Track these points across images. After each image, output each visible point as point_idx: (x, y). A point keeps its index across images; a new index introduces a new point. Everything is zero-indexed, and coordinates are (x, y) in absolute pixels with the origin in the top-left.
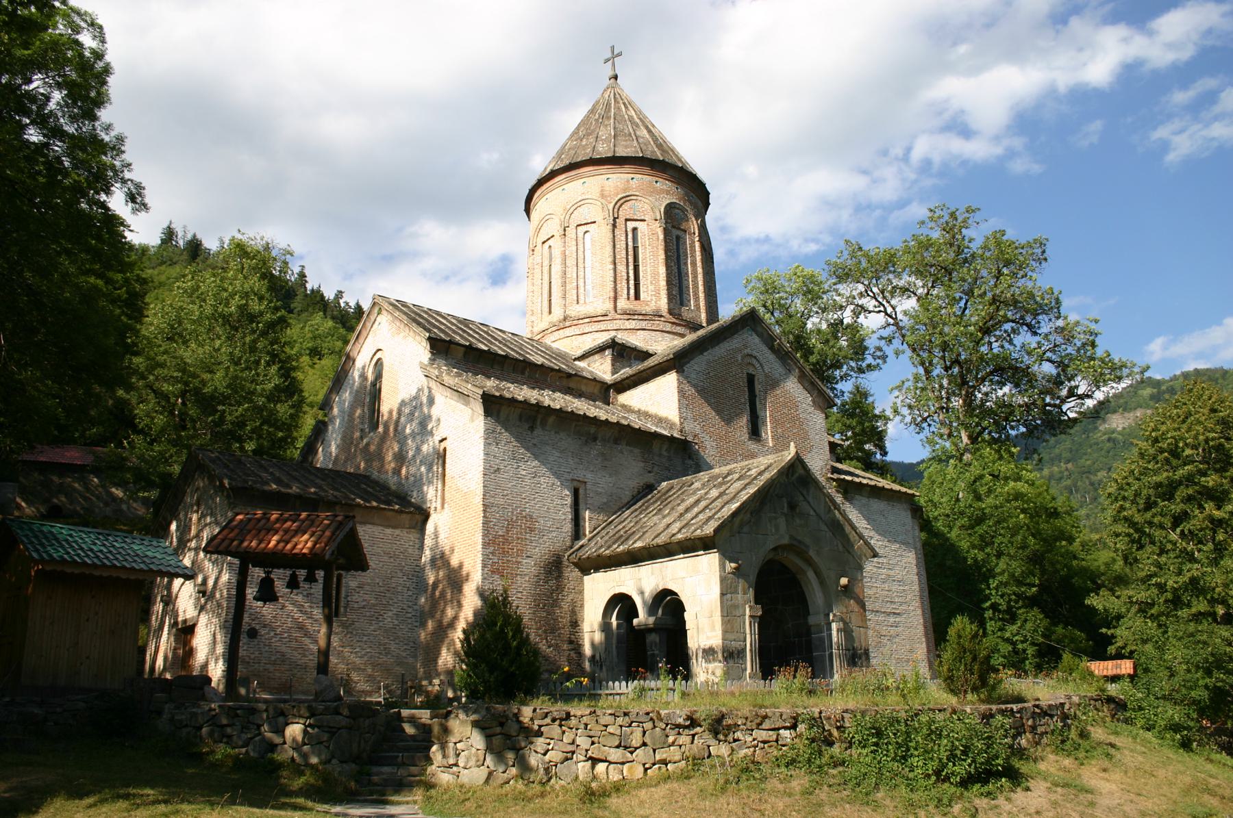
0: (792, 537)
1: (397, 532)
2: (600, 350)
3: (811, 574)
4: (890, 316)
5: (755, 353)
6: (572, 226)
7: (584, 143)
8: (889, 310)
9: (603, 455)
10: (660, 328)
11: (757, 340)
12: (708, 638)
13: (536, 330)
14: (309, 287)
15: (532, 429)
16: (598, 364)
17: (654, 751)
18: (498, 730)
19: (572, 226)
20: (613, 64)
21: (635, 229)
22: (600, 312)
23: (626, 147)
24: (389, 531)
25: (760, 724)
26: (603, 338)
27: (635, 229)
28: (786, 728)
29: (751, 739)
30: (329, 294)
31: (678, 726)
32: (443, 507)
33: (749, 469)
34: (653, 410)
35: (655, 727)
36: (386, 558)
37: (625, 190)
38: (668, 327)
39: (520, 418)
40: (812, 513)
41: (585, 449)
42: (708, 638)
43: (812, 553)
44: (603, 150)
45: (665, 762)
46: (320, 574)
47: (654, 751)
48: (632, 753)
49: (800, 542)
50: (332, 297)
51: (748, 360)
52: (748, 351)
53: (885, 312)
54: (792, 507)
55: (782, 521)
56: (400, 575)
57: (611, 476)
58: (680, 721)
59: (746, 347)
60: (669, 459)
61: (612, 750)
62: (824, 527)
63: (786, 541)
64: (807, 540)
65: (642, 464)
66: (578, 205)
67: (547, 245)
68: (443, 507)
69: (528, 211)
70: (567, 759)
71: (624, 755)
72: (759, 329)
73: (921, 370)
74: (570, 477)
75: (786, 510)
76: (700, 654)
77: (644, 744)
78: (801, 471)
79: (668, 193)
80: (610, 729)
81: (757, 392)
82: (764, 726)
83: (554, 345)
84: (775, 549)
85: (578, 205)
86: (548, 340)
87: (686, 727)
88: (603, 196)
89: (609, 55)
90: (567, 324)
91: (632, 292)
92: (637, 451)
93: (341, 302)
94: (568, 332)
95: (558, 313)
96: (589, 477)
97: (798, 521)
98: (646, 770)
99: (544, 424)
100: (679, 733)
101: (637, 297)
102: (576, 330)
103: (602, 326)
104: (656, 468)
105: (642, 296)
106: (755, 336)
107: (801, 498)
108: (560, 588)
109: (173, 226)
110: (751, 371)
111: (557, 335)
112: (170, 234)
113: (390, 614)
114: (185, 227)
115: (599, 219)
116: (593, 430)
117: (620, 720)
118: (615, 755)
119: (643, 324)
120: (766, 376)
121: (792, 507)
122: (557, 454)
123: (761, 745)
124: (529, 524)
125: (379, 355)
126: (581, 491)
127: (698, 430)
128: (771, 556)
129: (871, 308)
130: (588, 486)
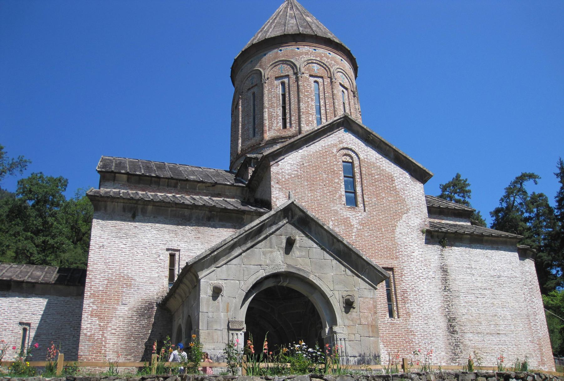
1: (68, 299)
5: (350, 146)
24: (61, 298)
39: (124, 209)
49: (299, 269)
51: (345, 151)
72: (355, 128)
74: (166, 247)
79: (307, 54)
91: (281, 124)
96: (182, 246)
99: (144, 212)
116: (187, 212)
122: (155, 232)
124: (127, 282)
126: (177, 257)
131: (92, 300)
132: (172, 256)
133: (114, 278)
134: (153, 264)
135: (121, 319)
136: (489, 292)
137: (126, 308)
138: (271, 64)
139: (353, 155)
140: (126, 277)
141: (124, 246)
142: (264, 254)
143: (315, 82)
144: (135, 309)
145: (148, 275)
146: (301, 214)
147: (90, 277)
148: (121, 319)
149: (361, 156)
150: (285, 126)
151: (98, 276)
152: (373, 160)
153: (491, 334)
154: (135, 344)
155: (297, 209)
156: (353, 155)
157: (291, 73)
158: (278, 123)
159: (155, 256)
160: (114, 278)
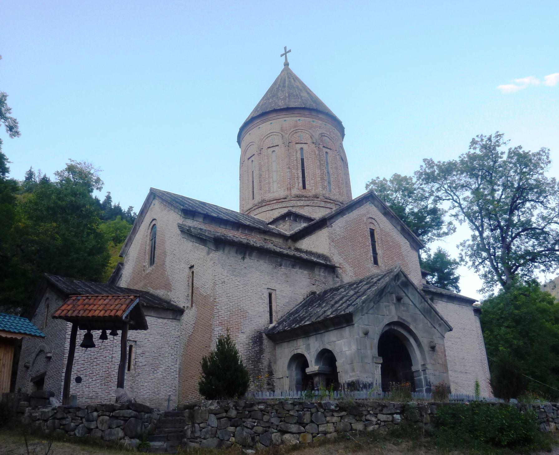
0: (399, 317)
1: (165, 321)
2: (283, 218)
3: (412, 341)
4: (456, 202)
5: (374, 217)
6: (265, 148)
7: (271, 101)
8: (455, 197)
9: (285, 274)
10: (318, 205)
11: (375, 209)
12: (351, 377)
13: (245, 209)
14: (113, 204)
15: (243, 258)
16: (281, 226)
17: (318, 426)
18: (224, 415)
19: (265, 148)
20: (286, 57)
21: (302, 149)
22: (282, 196)
23: (295, 102)
25: (382, 410)
26: (285, 211)
27: (302, 149)
28: (397, 413)
29: (376, 420)
30: (125, 208)
31: (333, 411)
32: (192, 306)
33: (372, 279)
34: (314, 250)
35: (318, 411)
36: (158, 337)
37: (295, 127)
38: (323, 204)
40: (411, 303)
41: (276, 271)
42: (351, 377)
43: (412, 327)
44: (281, 104)
45: (325, 433)
46: (120, 332)
47: (318, 426)
48: (304, 427)
49: (404, 320)
50: (126, 210)
51: (370, 220)
52: (370, 216)
53: (453, 199)
54: (399, 299)
55: (393, 308)
56: (167, 346)
57: (290, 286)
58: (333, 407)
59: (368, 213)
60: (325, 277)
61: (293, 425)
62: (419, 312)
63: (396, 319)
64: (409, 320)
65: (309, 280)
66: (268, 136)
67: (250, 160)
68: (192, 306)
69: (239, 142)
70: (266, 431)
71: (299, 428)
73: (477, 233)
75: (395, 301)
76: (346, 386)
77: (312, 422)
78: (403, 279)
79: (320, 127)
80: (291, 413)
81: (376, 240)
82: (384, 412)
83: (255, 217)
84: (389, 324)
85: (268, 136)
86: (252, 215)
87: (336, 411)
88: (282, 130)
89: (284, 52)
90: (264, 204)
91: (301, 185)
92: (306, 272)
93: (132, 212)
94: (264, 209)
95: (258, 199)
96: (277, 287)
97: (402, 308)
98: (313, 437)
100: (333, 416)
101: (304, 187)
102: (269, 208)
103: (284, 205)
104: (317, 283)
105: (307, 186)
106: (373, 207)
107: (404, 295)
108: (261, 351)
109: (32, 170)
110: (372, 227)
111: (257, 211)
112: (30, 175)
113: (161, 369)
114: (39, 170)
115: (280, 143)
117: (297, 408)
118: (294, 428)
119: (308, 203)
120: (381, 230)
121: (399, 299)
122: (259, 273)
123: (383, 424)
125: (154, 222)
126: (273, 296)
127: (341, 261)
128: (387, 328)
129: (444, 198)
130: (277, 293)
131: (220, 328)
132: (270, 295)
133: (234, 310)
134: (260, 301)
135: (241, 345)
136: (459, 340)
137: (245, 336)
138: (292, 130)
139: (376, 224)
140: (242, 310)
141: (238, 283)
142: (386, 307)
143: (327, 153)
144: (250, 337)
145: (257, 309)
146: (404, 279)
147: (218, 308)
148: (241, 345)
149: (381, 225)
150: (304, 187)
151: (223, 308)
152: (388, 230)
153: (462, 372)
154: (253, 367)
155: (402, 275)
156: (376, 224)
157: (309, 141)
158: (299, 183)
159: (260, 293)
160: (234, 310)
